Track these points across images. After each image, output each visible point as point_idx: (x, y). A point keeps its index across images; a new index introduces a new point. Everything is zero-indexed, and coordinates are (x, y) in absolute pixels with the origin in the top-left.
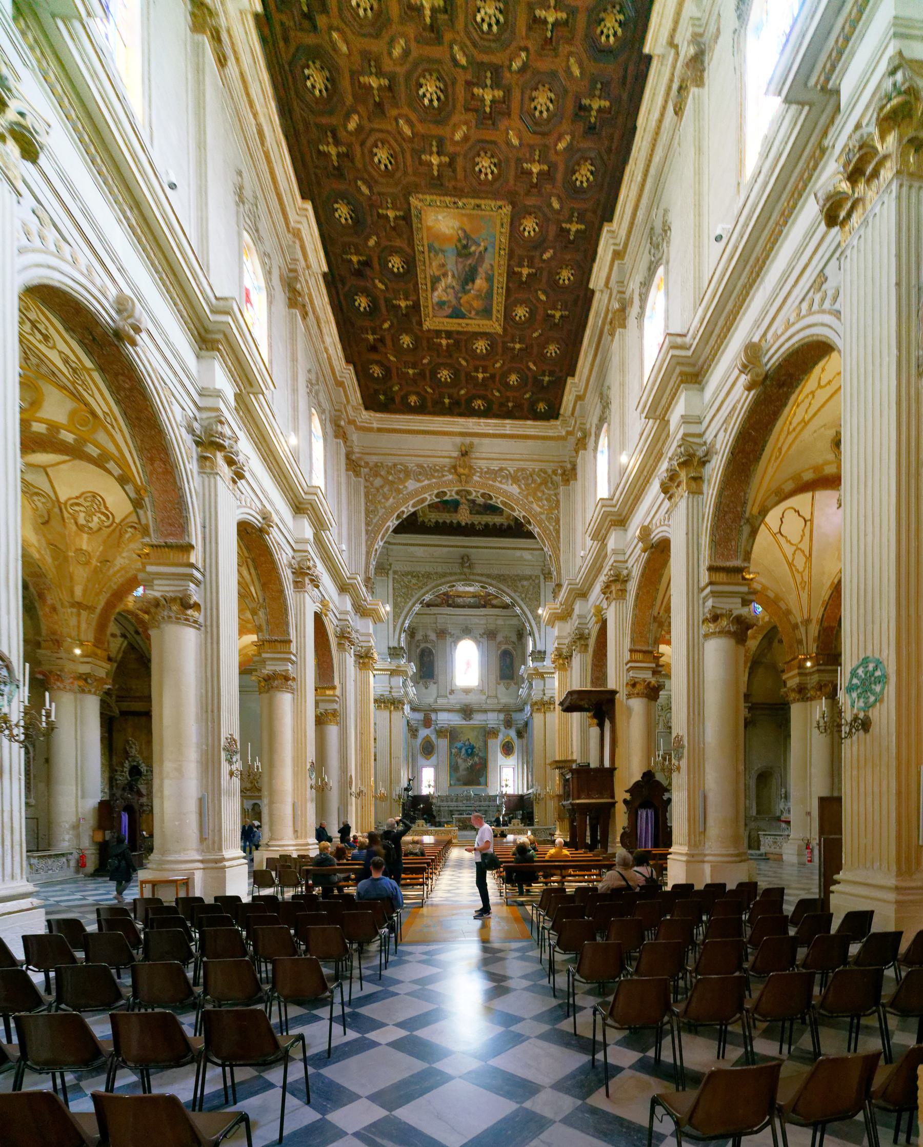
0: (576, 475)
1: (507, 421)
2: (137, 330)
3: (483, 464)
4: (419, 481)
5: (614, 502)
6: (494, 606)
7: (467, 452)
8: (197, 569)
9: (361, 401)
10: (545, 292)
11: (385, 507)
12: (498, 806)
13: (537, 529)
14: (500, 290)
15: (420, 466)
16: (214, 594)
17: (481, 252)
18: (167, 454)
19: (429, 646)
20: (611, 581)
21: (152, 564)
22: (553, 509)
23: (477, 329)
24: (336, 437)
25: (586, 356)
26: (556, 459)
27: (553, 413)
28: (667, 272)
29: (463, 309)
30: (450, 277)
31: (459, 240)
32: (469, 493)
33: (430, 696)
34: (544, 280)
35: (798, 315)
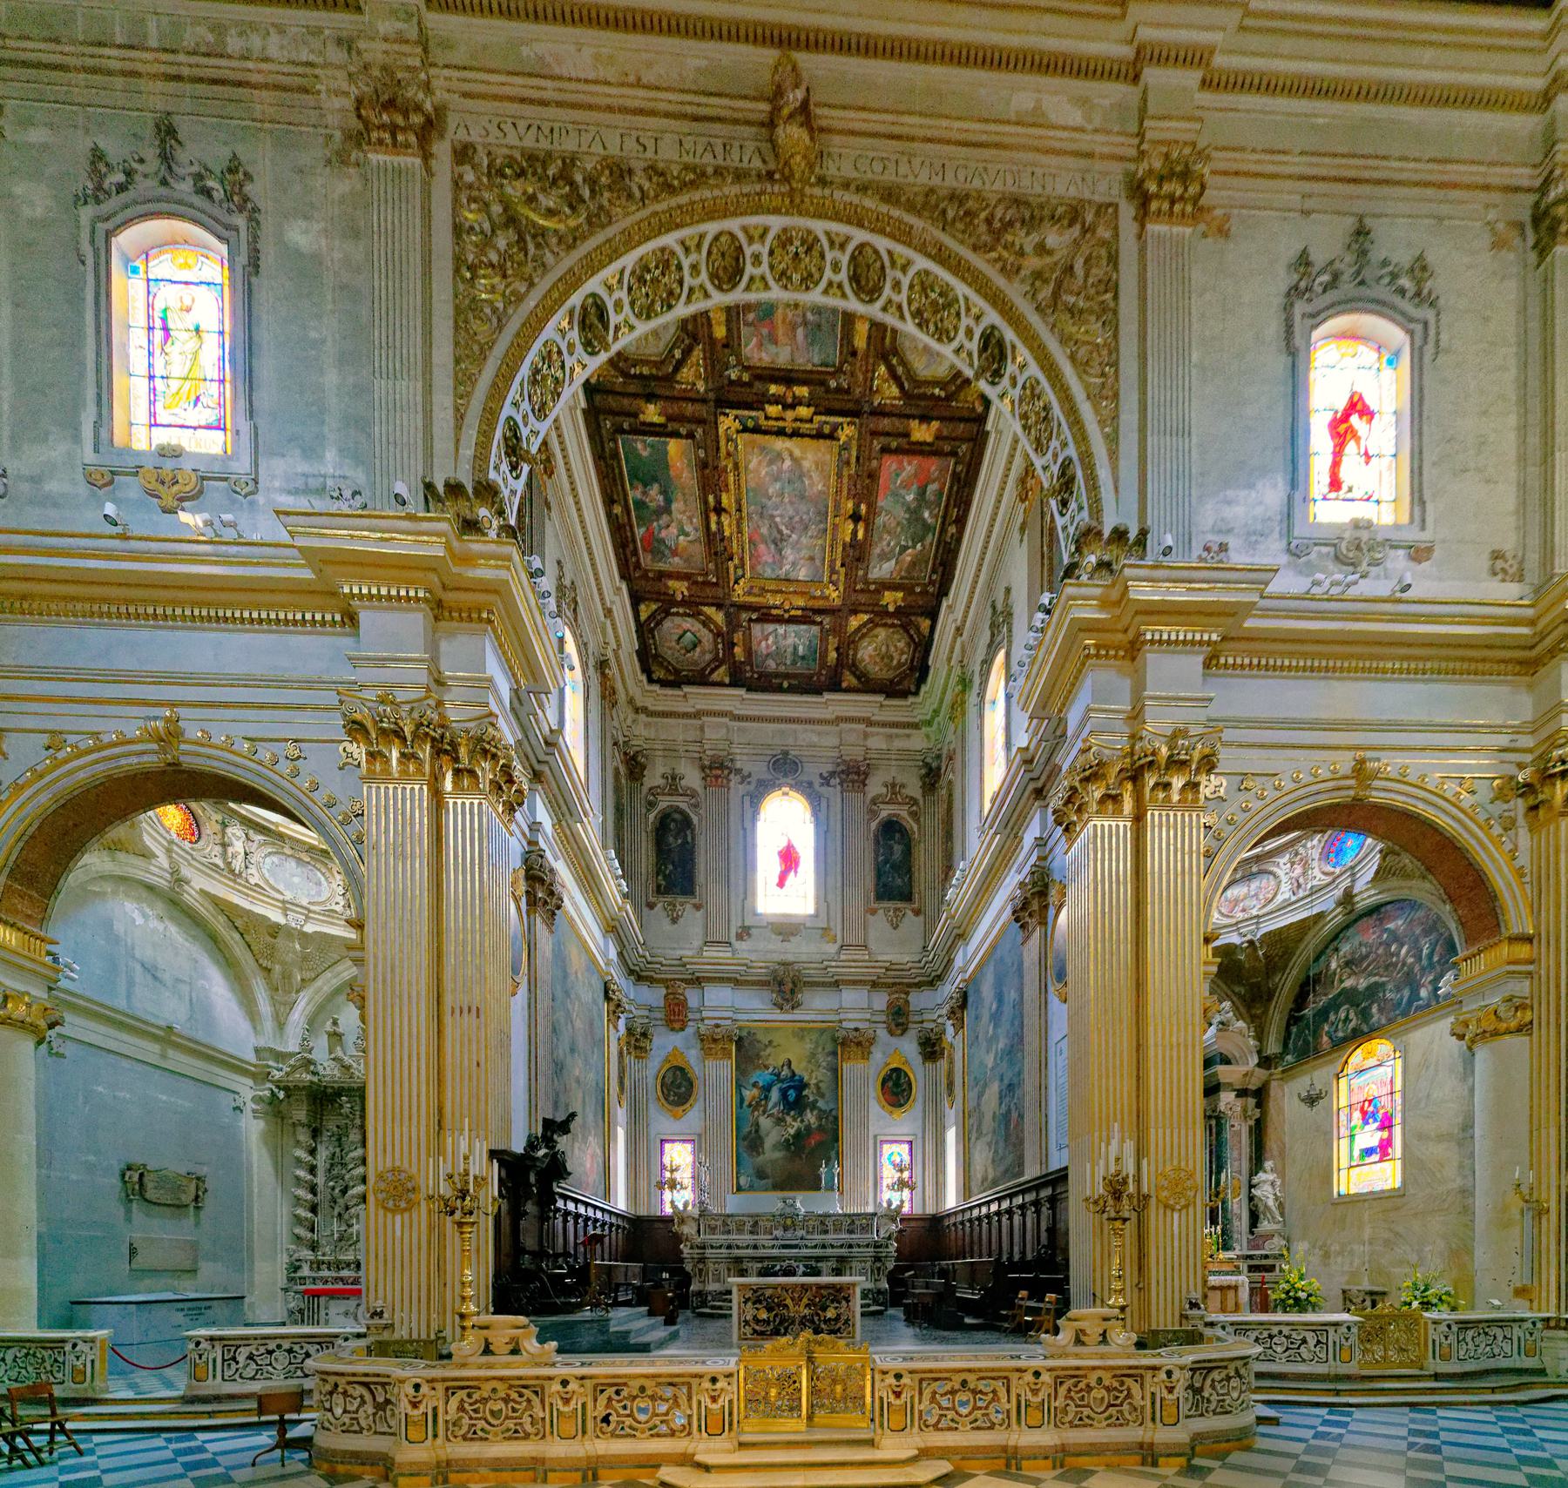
19: (682, 803)
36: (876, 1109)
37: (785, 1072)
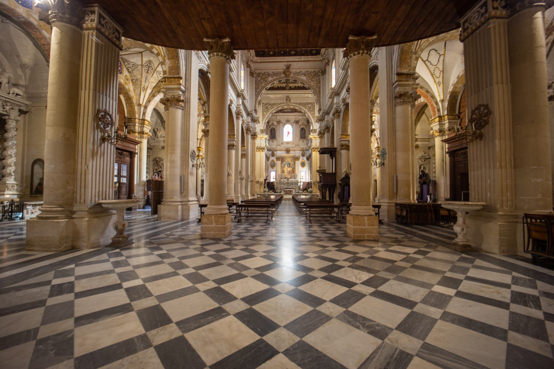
0: (326, 72)
1: (303, 57)
3: (294, 70)
4: (272, 77)
9: (255, 55)
15: (273, 73)
26: (319, 67)
33: (274, 145)
36: (300, 167)
37: (288, 163)
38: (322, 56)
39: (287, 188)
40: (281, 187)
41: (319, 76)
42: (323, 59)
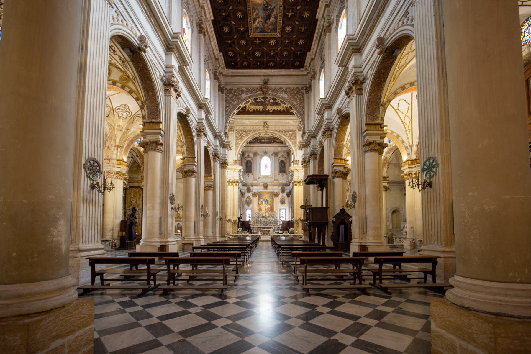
0: (311, 89)
1: (283, 70)
2: (146, 47)
3: (273, 87)
4: (247, 94)
5: (326, 99)
6: (278, 143)
7: (266, 82)
8: (162, 130)
9: (225, 65)
10: (298, 21)
11: (233, 105)
12: (278, 226)
13: (295, 111)
14: (280, 21)
15: (248, 89)
16: (168, 140)
17: (272, 8)
18: (154, 89)
19: (250, 159)
20: (326, 131)
21: (146, 129)
22: (302, 103)
23: (271, 36)
24: (215, 79)
25: (315, 43)
26: (302, 83)
27: (301, 66)
28: (347, 12)
29: (265, 29)
30: (260, 18)
31: (264, 5)
32: (267, 98)
33: (250, 179)
34: (298, 17)
35: (398, 26)
37: (265, 199)
38: (306, 69)
39: (264, 228)
40: (258, 227)
41: (303, 94)
42: (308, 73)
